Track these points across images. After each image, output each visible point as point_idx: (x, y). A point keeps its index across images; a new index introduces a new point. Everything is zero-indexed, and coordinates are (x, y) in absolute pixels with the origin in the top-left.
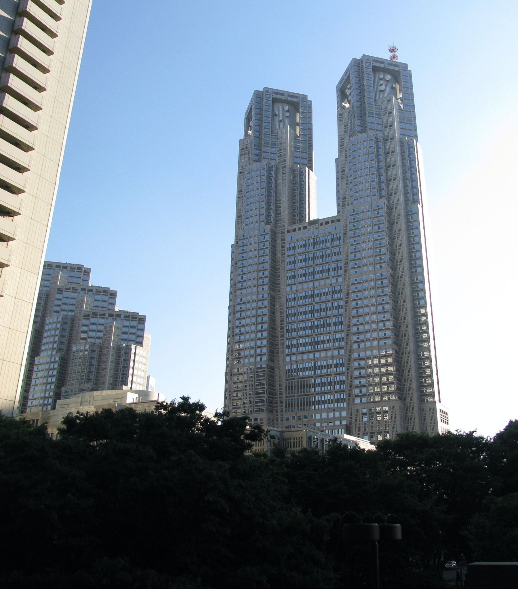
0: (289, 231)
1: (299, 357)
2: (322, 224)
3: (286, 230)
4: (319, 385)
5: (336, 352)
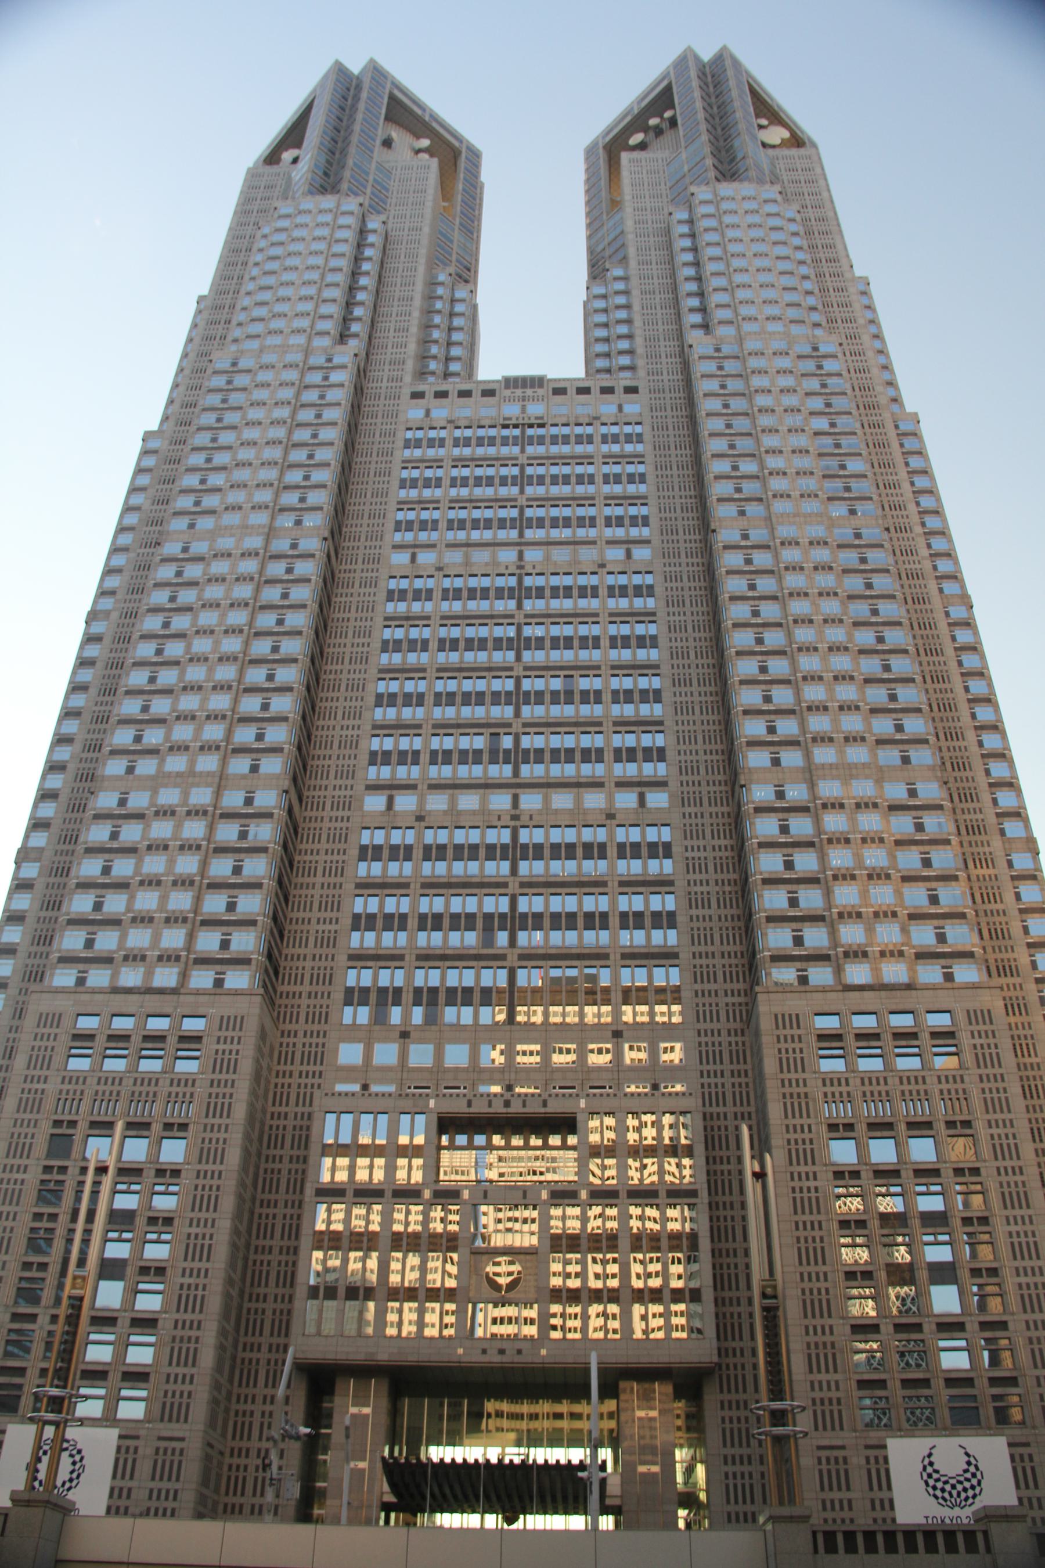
0: (417, 395)
1: (437, 802)
2: (560, 391)
3: (407, 392)
4: (537, 921)
5: (627, 800)
